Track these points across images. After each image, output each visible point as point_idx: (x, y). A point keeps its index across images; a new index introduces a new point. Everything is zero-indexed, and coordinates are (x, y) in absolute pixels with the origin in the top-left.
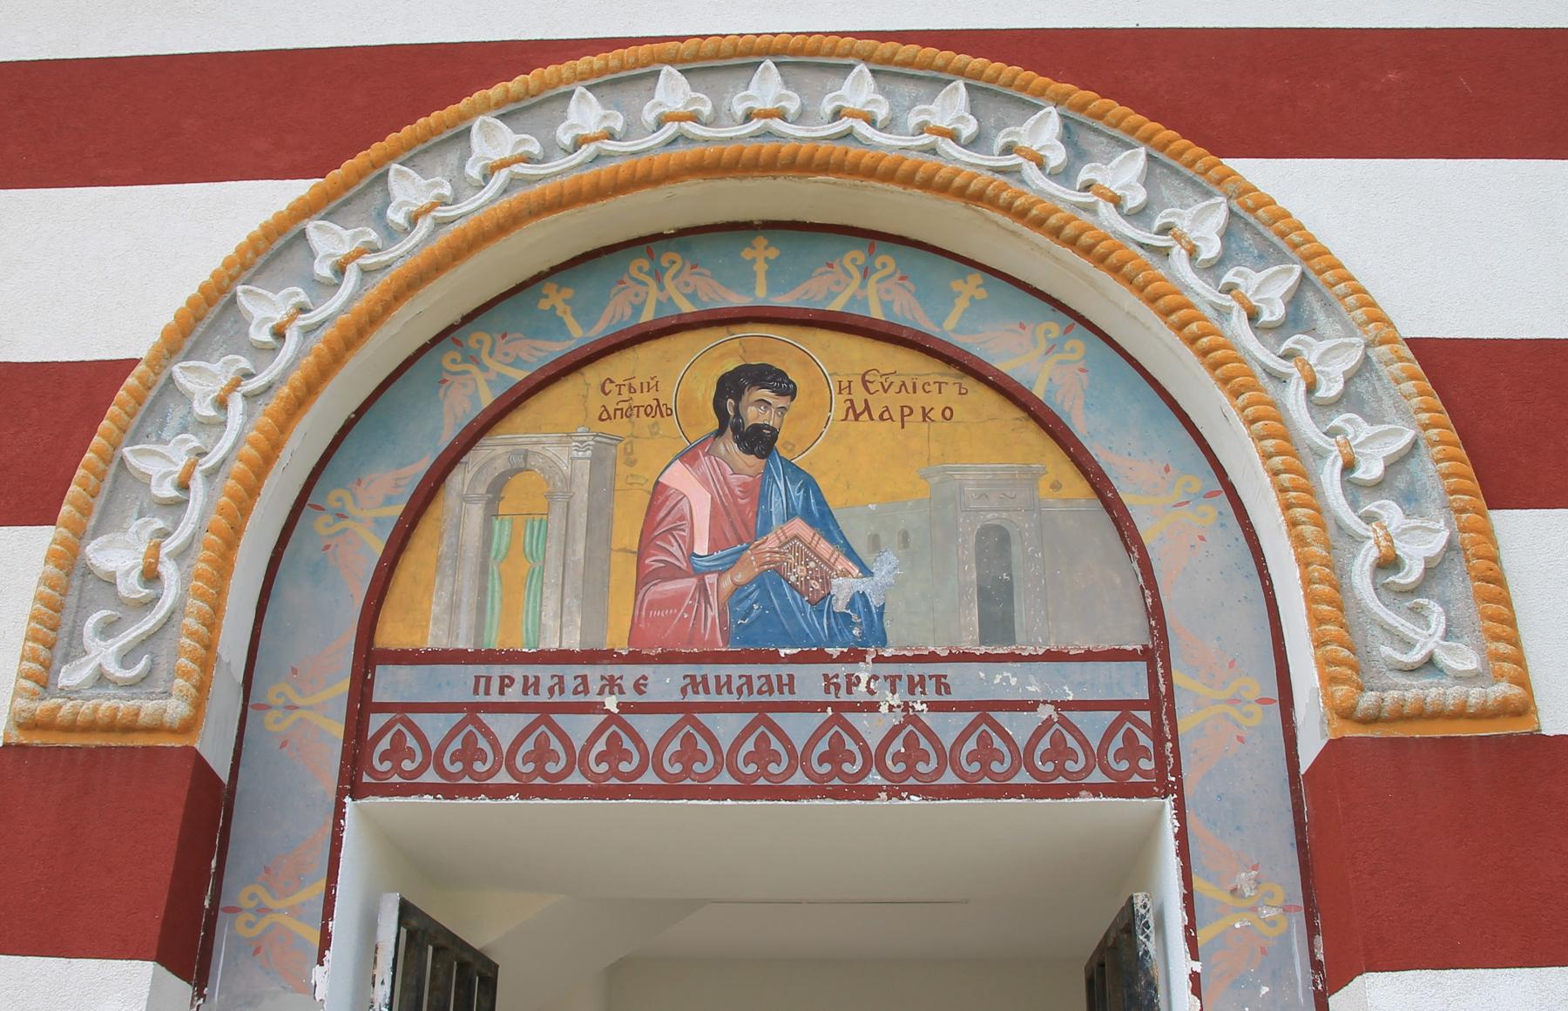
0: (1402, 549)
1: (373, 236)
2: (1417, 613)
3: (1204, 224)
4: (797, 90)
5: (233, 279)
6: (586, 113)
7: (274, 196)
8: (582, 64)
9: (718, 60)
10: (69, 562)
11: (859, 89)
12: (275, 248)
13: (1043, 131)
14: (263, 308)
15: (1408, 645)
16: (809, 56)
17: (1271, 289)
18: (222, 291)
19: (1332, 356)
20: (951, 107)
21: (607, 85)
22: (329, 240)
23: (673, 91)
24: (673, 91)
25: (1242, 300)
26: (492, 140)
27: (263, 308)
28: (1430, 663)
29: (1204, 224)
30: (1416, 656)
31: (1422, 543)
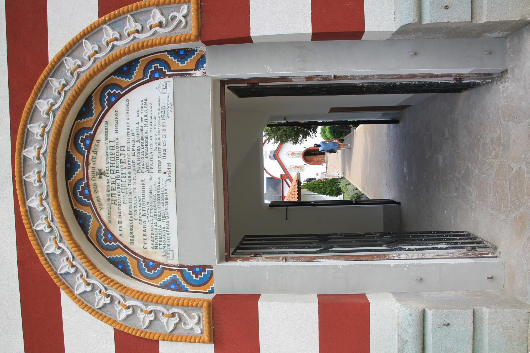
0: (157, 21)
1: (79, 275)
2: (173, 18)
4: (32, 169)
5: (94, 310)
8: (26, 226)
9: (21, 190)
10: (171, 337)
11: (31, 153)
15: (181, 21)
18: (98, 313)
20: (36, 129)
21: (32, 220)
25: (93, 55)
26: (50, 248)
27: (100, 300)
28: (185, 17)
30: (183, 20)
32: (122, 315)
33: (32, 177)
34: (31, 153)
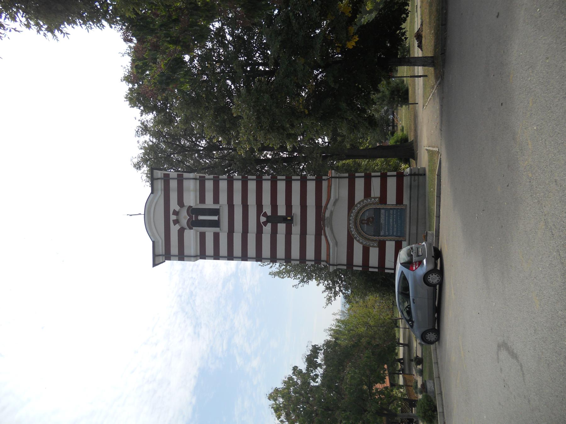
3: (359, 205)
6: (352, 229)
7: (355, 241)
11: (351, 218)
12: (358, 241)
13: (354, 211)
14: (361, 241)
16: (349, 220)
17: (362, 203)
19: (365, 201)
20: (352, 214)
22: (358, 239)
23: (351, 226)
24: (351, 226)
26: (353, 233)
29: (359, 205)
31: (373, 200)
32: (364, 243)
33: (351, 222)
34: (351, 218)
